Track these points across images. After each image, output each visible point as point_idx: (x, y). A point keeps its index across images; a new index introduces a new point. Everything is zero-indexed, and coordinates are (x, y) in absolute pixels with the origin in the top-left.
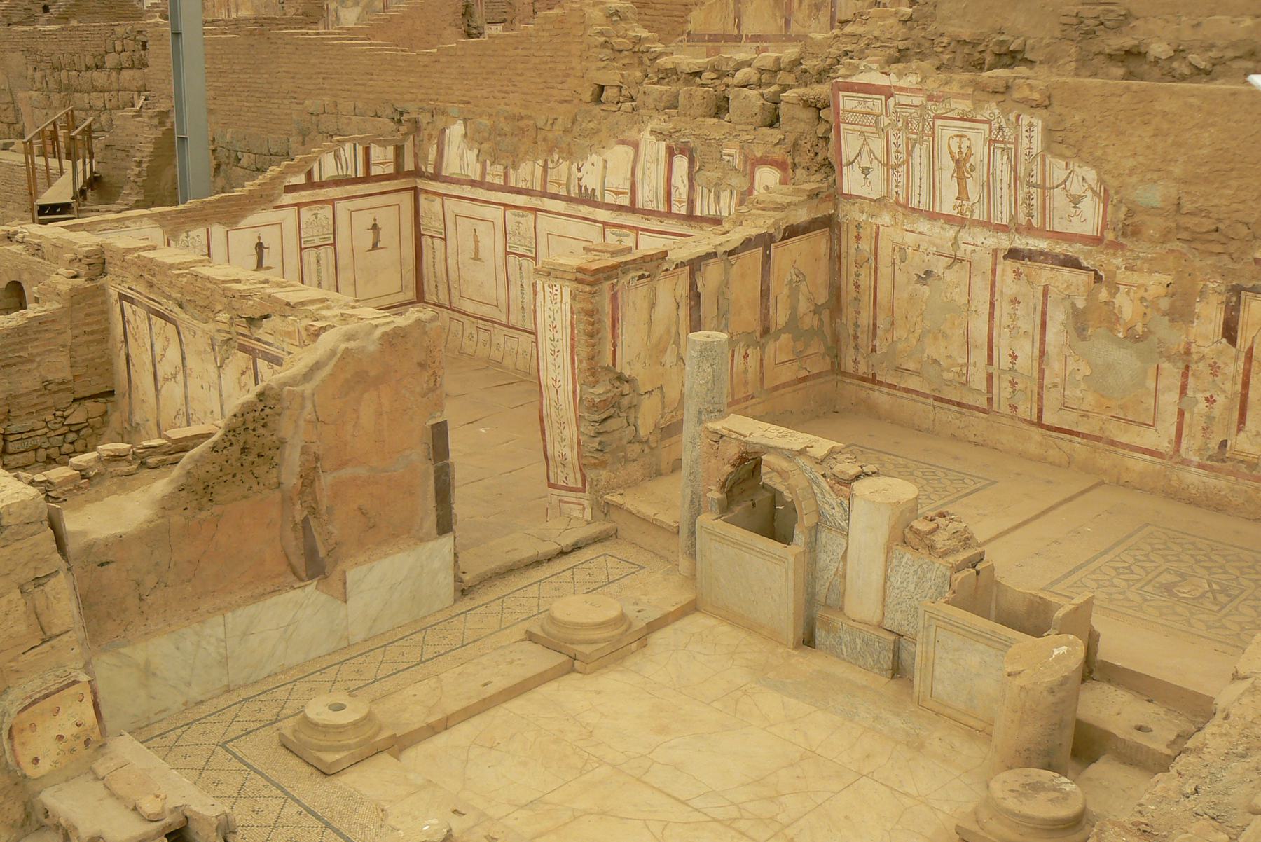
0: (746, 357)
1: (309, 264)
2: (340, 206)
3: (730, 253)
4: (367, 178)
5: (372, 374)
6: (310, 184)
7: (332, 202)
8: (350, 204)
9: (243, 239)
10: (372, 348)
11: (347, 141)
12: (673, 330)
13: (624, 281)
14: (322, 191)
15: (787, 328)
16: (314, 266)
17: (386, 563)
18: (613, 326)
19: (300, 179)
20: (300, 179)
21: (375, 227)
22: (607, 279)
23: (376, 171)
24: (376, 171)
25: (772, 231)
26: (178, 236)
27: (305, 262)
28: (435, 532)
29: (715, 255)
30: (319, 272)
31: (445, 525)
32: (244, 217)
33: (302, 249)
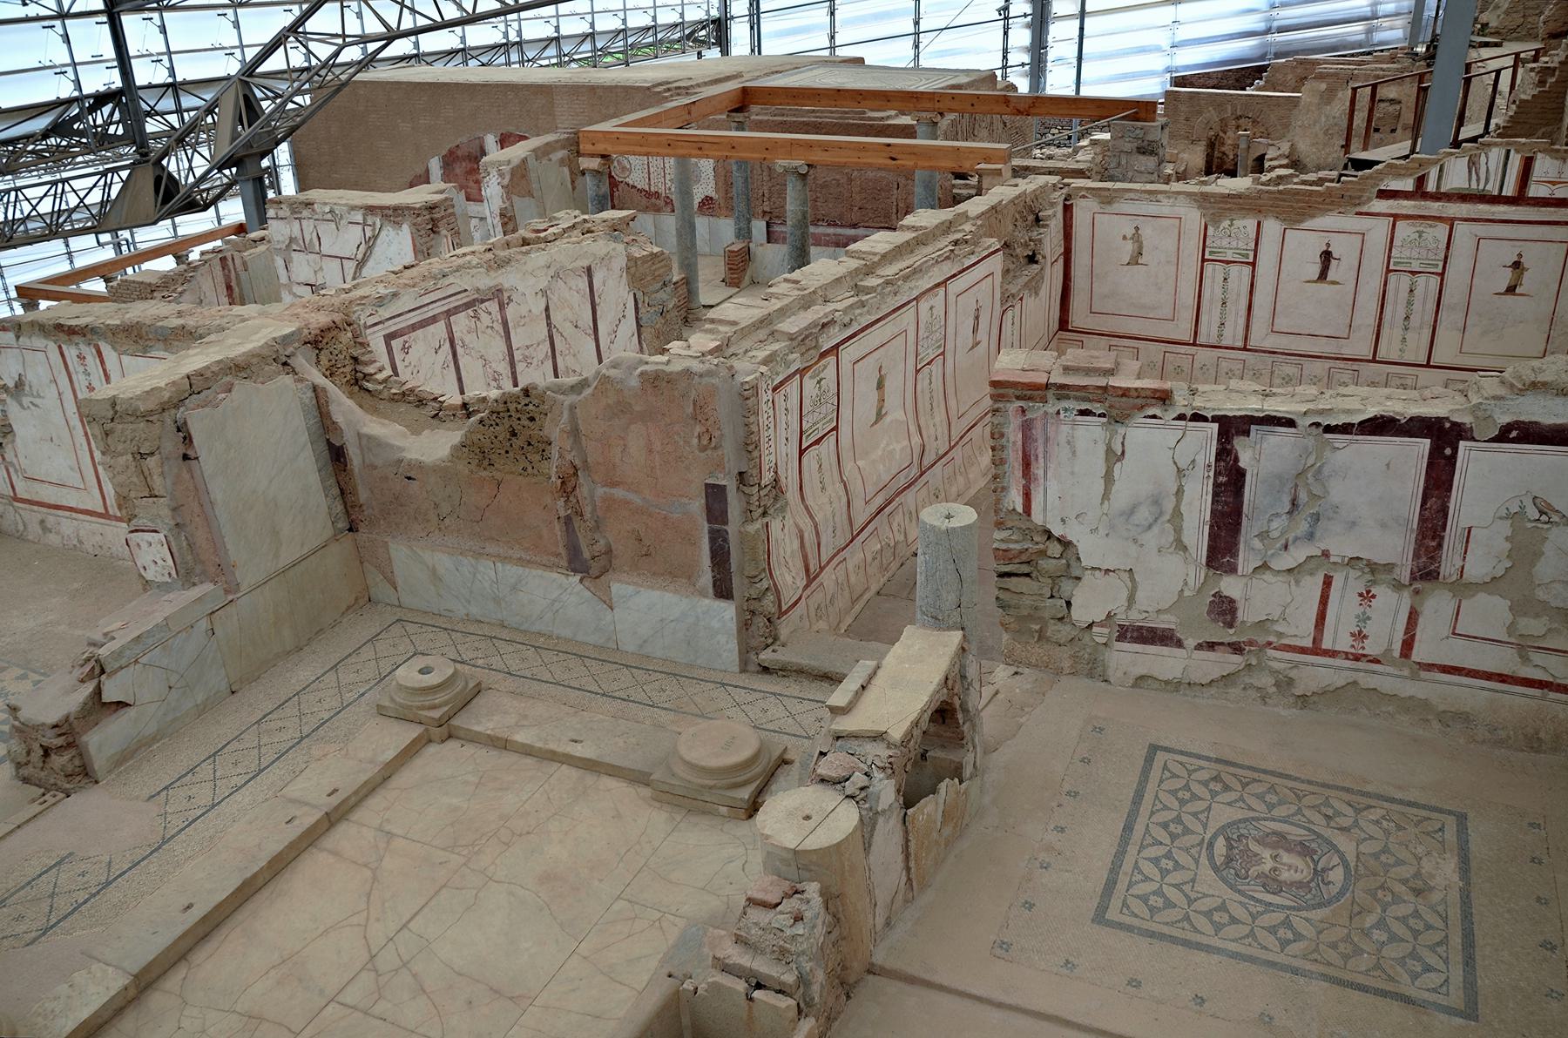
0: (1367, 596)
1: (1397, 290)
2: (1460, 228)
3: (1329, 429)
4: (1520, 199)
5: (637, 408)
6: (1420, 192)
7: (1451, 222)
8: (1480, 229)
9: (1304, 244)
10: (634, 382)
11: (1496, 144)
12: (1169, 505)
13: (1051, 407)
14: (1437, 204)
15: (1491, 585)
16: (1404, 294)
17: (655, 595)
18: (1027, 465)
19: (1408, 185)
20: (1408, 185)
21: (1517, 265)
22: (1018, 398)
23: (1534, 191)
24: (1534, 191)
25: (1466, 420)
26: (1220, 222)
27: (1391, 287)
28: (711, 591)
29: (1291, 423)
30: (1410, 303)
31: (723, 590)
32: (1313, 216)
33: (1388, 271)
